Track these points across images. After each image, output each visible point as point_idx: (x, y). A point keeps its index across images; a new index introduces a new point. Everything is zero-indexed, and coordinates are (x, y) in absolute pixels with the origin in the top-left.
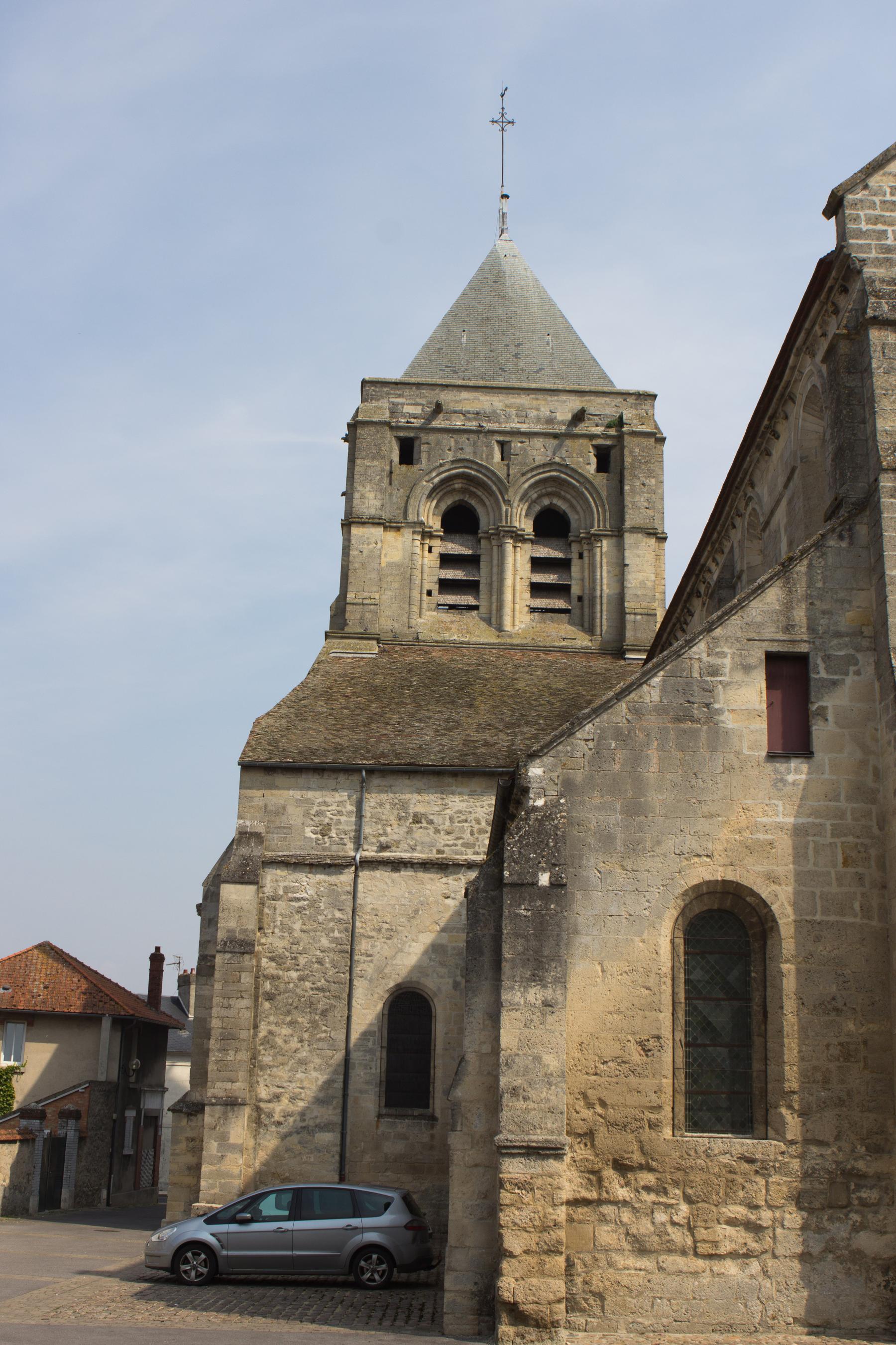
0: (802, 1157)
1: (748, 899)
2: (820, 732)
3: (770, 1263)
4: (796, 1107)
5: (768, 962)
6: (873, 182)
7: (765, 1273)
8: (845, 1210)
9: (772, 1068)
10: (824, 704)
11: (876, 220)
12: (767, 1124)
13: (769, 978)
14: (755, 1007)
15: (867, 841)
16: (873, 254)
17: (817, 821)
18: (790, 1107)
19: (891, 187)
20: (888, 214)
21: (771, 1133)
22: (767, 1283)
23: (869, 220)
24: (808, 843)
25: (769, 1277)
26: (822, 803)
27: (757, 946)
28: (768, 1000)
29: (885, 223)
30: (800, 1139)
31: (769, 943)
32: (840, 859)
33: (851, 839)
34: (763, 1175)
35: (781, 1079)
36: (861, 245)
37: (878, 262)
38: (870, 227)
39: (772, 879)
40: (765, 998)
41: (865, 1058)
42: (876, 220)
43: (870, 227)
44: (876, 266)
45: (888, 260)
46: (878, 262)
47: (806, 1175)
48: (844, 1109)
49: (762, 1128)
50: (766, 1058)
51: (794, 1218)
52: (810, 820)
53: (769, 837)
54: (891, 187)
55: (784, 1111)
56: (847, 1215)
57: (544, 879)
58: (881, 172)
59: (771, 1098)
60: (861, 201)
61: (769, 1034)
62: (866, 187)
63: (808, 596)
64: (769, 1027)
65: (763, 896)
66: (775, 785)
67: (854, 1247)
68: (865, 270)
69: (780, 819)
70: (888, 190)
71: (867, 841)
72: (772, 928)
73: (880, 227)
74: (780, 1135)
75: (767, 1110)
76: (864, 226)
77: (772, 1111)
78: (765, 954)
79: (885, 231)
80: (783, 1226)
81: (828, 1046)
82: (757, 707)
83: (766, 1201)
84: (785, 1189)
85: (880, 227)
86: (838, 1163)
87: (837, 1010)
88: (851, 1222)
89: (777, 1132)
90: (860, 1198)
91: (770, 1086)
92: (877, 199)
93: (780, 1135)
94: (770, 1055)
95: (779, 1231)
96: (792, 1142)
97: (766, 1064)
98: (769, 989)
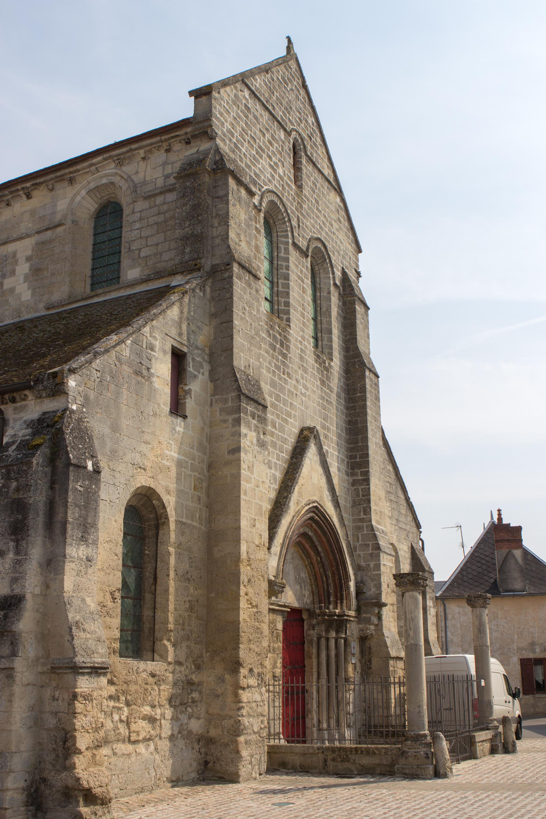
0: (173, 672)
1: (154, 502)
2: (190, 405)
3: (159, 743)
4: (173, 641)
5: (159, 545)
7: (156, 749)
8: (185, 706)
9: (158, 614)
10: (191, 388)
12: (153, 651)
13: (159, 555)
14: (147, 574)
15: (202, 477)
17: (186, 459)
18: (169, 640)
21: (156, 657)
22: (157, 757)
24: (182, 472)
25: (158, 753)
26: (188, 448)
27: (151, 533)
28: (158, 570)
30: (173, 661)
31: (161, 532)
32: (193, 487)
33: (196, 474)
34: (157, 685)
35: (167, 622)
39: (168, 492)
40: (156, 568)
41: (197, 610)
47: (175, 684)
48: (189, 642)
49: (150, 654)
50: (155, 608)
51: (169, 713)
52: (183, 458)
53: (168, 464)
55: (166, 642)
56: (186, 709)
57: (90, 465)
59: (157, 634)
61: (158, 592)
63: (188, 319)
64: (158, 588)
65: (164, 501)
66: (171, 431)
67: (189, 729)
69: (172, 454)
71: (202, 477)
72: (164, 523)
74: (164, 658)
75: (154, 642)
77: (158, 643)
78: (157, 539)
80: (164, 718)
81: (185, 602)
82: (167, 378)
83: (158, 702)
84: (166, 693)
86: (186, 676)
87: (188, 579)
88: (188, 713)
89: (161, 656)
90: (192, 698)
91: (157, 627)
93: (164, 658)
94: (157, 606)
95: (163, 721)
96: (170, 663)
97: (154, 612)
98: (159, 563)
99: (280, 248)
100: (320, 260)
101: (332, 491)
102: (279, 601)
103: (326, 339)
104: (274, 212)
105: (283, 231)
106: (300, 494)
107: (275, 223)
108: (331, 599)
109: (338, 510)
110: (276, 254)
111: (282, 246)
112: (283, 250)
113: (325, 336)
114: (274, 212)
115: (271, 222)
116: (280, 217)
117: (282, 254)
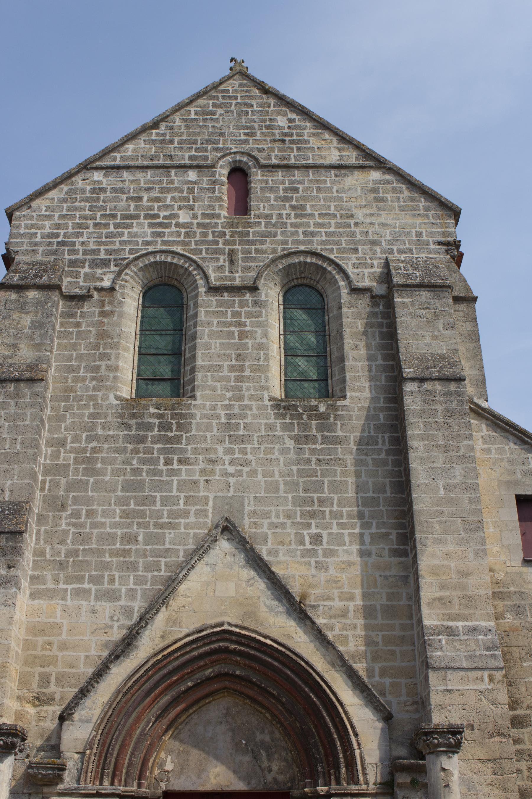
6: (34, 204)
11: (32, 227)
16: (25, 247)
19: (46, 207)
20: (40, 223)
23: (26, 227)
29: (37, 228)
36: (18, 242)
37: (27, 252)
38: (27, 231)
42: (32, 227)
43: (27, 231)
44: (24, 255)
45: (33, 250)
46: (27, 252)
54: (46, 207)
58: (42, 198)
60: (24, 216)
62: (30, 207)
68: (17, 257)
70: (44, 208)
73: (33, 231)
76: (22, 231)
79: (36, 233)
85: (33, 231)
92: (35, 214)
99: (190, 305)
100: (317, 274)
101: (285, 597)
102: (79, 789)
103: (337, 373)
104: (169, 271)
105: (192, 285)
106: (172, 621)
107: (179, 282)
108: (319, 769)
109: (308, 622)
110: (185, 316)
111: (191, 303)
112: (192, 306)
113: (336, 369)
114: (169, 271)
115: (176, 283)
116: (181, 271)
117: (191, 312)
